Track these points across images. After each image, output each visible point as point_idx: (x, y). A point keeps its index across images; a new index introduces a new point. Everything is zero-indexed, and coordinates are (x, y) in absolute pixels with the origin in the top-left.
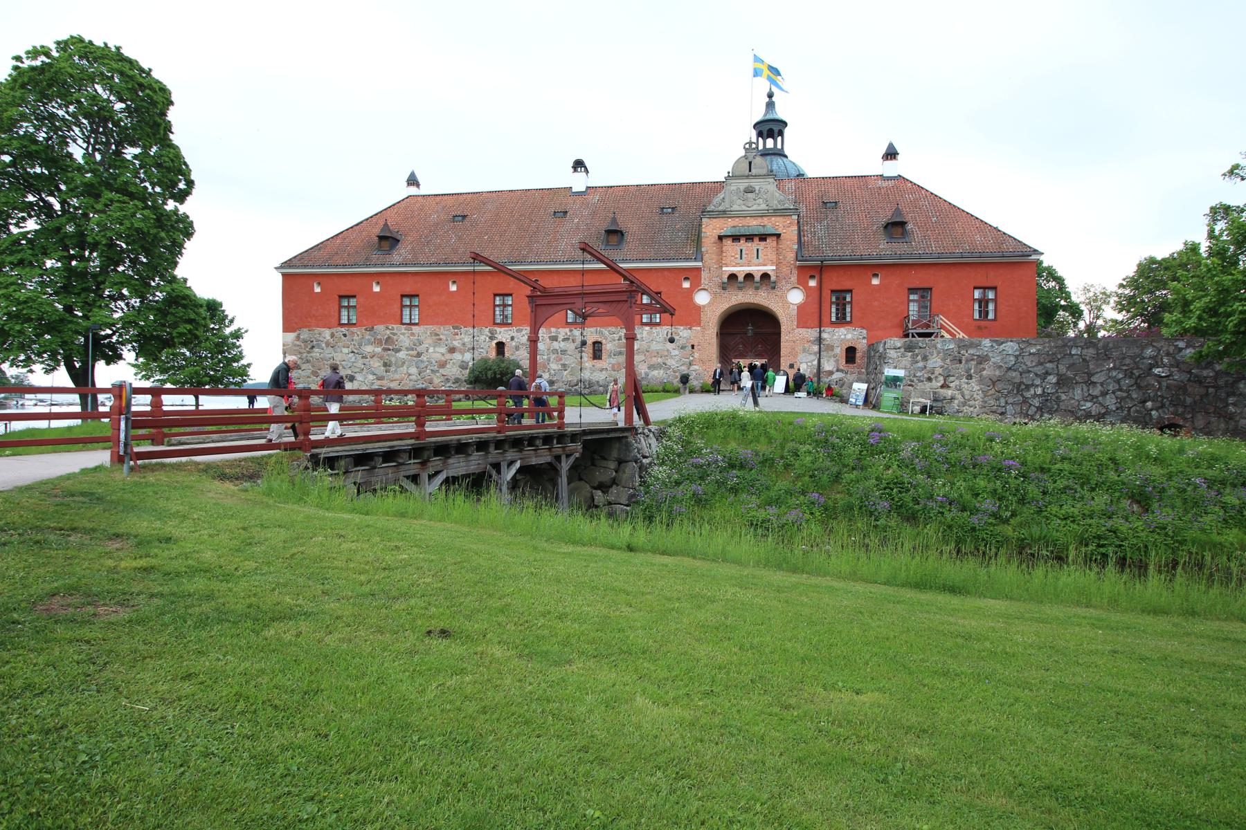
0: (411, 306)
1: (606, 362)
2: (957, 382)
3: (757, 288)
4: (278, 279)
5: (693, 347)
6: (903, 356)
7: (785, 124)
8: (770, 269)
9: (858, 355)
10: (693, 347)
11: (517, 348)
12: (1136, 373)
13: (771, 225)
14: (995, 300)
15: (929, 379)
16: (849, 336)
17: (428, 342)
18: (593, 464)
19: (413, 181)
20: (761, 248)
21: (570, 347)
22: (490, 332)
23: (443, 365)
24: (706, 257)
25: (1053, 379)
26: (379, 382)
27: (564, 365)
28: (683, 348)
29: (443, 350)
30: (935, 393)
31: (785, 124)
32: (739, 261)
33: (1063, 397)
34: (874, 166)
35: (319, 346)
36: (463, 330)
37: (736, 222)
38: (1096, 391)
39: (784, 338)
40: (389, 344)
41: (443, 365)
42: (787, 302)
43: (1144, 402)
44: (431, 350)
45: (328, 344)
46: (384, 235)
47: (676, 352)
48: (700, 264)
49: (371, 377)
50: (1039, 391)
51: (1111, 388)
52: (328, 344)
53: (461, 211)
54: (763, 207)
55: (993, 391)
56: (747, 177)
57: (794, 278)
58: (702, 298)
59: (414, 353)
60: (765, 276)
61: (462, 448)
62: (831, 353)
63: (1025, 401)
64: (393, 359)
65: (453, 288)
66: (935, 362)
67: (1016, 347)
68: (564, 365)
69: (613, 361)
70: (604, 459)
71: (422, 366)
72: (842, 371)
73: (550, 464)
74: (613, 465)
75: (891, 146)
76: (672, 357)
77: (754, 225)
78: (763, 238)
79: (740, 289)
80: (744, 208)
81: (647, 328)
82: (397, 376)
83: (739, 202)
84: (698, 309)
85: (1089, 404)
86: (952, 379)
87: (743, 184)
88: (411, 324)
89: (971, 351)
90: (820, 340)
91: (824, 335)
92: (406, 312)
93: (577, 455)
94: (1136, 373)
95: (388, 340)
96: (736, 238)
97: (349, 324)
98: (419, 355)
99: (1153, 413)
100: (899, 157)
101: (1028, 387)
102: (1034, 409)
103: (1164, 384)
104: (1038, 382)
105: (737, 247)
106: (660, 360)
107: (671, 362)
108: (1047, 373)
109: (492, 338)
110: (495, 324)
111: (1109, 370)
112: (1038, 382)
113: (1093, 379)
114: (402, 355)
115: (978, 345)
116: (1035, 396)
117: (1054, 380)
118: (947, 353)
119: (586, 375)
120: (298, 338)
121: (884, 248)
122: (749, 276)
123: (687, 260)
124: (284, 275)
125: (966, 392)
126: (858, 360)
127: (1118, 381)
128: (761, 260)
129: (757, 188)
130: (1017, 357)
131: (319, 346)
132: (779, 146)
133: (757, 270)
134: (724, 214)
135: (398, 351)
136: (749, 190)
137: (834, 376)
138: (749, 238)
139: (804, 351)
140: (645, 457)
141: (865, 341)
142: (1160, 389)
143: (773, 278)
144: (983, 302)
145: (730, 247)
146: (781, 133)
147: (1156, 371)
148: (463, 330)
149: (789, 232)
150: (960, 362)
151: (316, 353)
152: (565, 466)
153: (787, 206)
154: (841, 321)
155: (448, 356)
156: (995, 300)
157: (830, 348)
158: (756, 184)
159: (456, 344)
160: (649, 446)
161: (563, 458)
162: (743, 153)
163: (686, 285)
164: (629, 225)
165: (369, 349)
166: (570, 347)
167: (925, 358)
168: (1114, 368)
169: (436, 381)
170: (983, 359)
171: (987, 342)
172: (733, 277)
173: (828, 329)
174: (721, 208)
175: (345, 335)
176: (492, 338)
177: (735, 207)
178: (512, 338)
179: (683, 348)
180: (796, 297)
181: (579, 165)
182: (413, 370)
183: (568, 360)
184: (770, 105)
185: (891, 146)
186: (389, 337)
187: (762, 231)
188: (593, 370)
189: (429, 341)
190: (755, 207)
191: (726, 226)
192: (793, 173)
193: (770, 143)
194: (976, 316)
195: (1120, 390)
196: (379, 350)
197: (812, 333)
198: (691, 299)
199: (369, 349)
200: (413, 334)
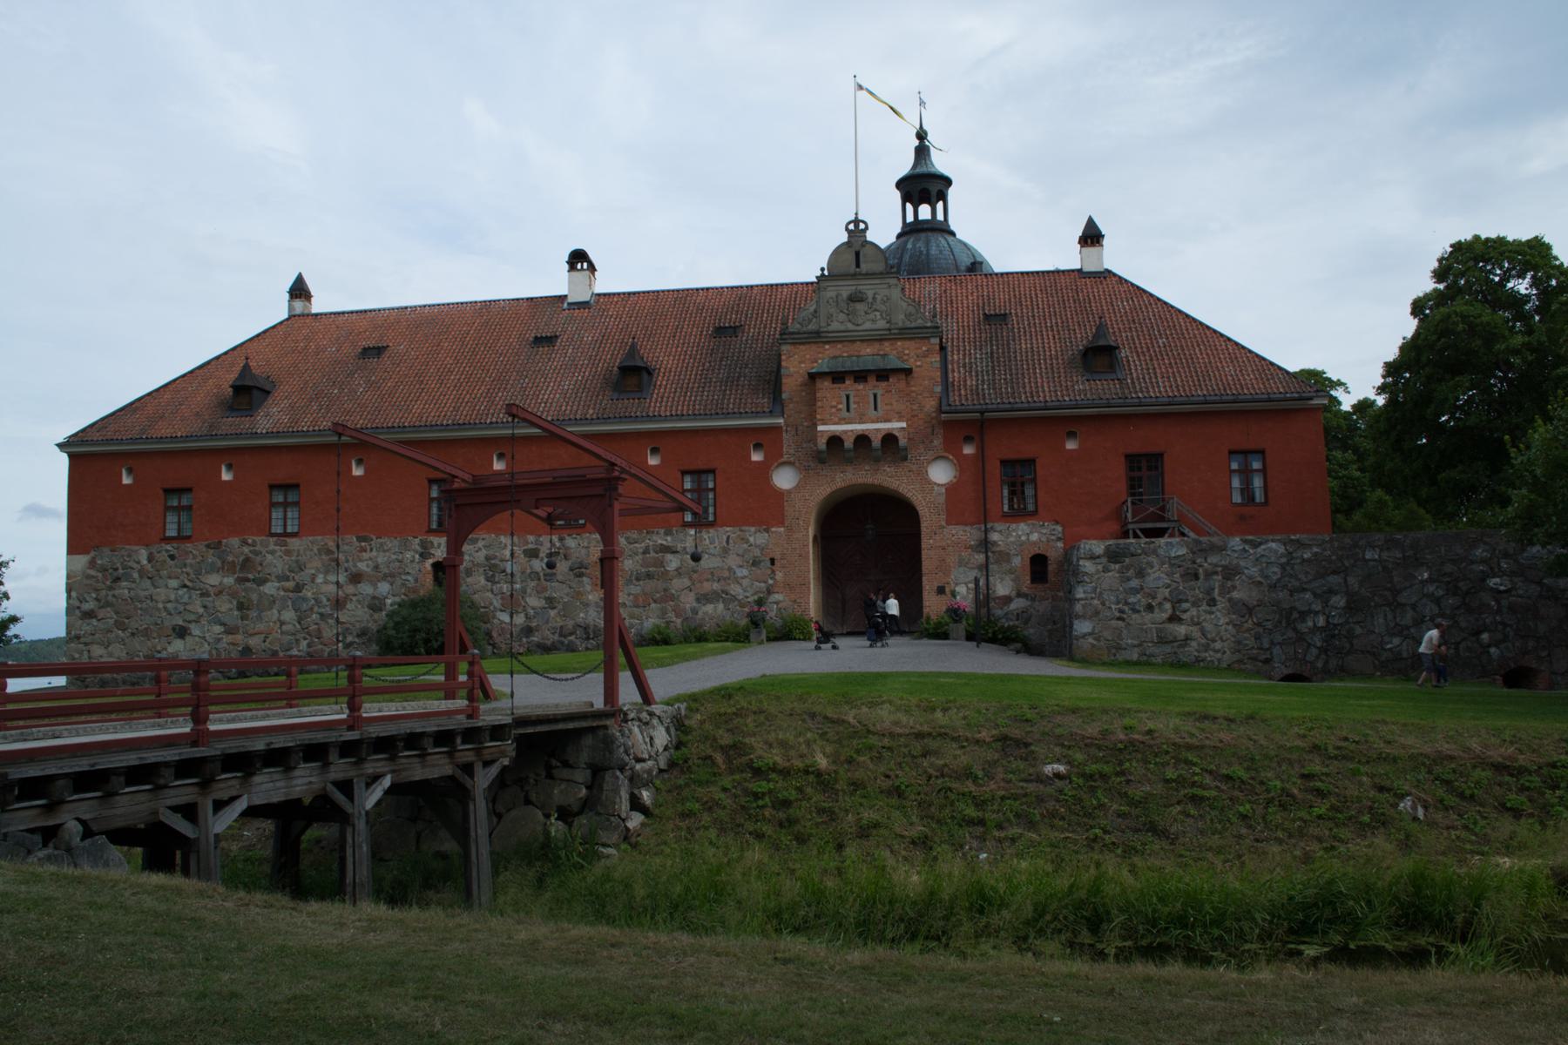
0: (285, 505)
2: (1194, 612)
3: (877, 460)
4: (63, 460)
5: (773, 561)
6: (1106, 570)
7: (948, 182)
8: (896, 425)
9: (1051, 568)
10: (773, 561)
12: (1463, 586)
13: (893, 353)
14: (1264, 471)
15: (1150, 608)
16: (1035, 537)
17: (314, 565)
18: (550, 776)
19: (299, 290)
20: (879, 392)
22: (423, 544)
23: (339, 604)
24: (790, 408)
25: (1339, 601)
26: (227, 639)
27: (551, 602)
28: (755, 563)
30: (1159, 631)
31: (948, 182)
32: (845, 414)
33: (1358, 630)
34: (1069, 257)
35: (128, 577)
36: (375, 542)
37: (838, 350)
38: (1408, 617)
39: (926, 542)
40: (247, 570)
42: (929, 482)
43: (1479, 633)
44: (320, 579)
45: (142, 573)
46: (241, 381)
47: (745, 572)
48: (781, 421)
49: (218, 629)
50: (1321, 621)
51: (1427, 612)
52: (142, 573)
53: (376, 340)
54: (882, 324)
55: (1249, 624)
56: (854, 276)
57: (938, 442)
58: (784, 479)
59: (291, 584)
60: (889, 439)
61: (278, 758)
62: (1005, 566)
63: (1300, 638)
64: (254, 597)
65: (357, 471)
66: (1158, 577)
67: (1282, 550)
68: (551, 602)
69: (635, 590)
70: (566, 764)
71: (305, 607)
72: (1025, 596)
73: (452, 778)
74: (581, 775)
75: (1091, 224)
76: (737, 581)
77: (868, 355)
78: (883, 375)
79: (849, 461)
80: (850, 326)
81: (692, 532)
82: (261, 627)
83: (842, 317)
84: (780, 495)
85: (1396, 641)
86: (1185, 605)
87: (846, 289)
88: (285, 534)
89: (1213, 559)
90: (985, 545)
91: (995, 537)
92: (277, 514)
93: (506, 762)
94: (1463, 586)
95: (247, 563)
96: (838, 377)
97: (181, 538)
98: (298, 588)
99: (1493, 650)
100: (1105, 242)
101: (1303, 615)
102: (1314, 651)
103: (1504, 603)
104: (1317, 607)
106: (716, 586)
107: (735, 589)
108: (1331, 592)
109: (424, 556)
110: (430, 531)
111: (1423, 582)
112: (1317, 607)
113: (1402, 599)
114: (270, 588)
115: (1222, 549)
116: (1316, 628)
117: (1342, 603)
118: (1174, 563)
120: (92, 564)
121: (1084, 390)
122: (862, 440)
123: (757, 414)
124: (72, 457)
125: (1208, 626)
126: (1051, 577)
127: (1438, 601)
128: (881, 412)
129: (870, 294)
130: (1283, 566)
131: (128, 577)
132: (940, 217)
133: (875, 427)
134: (816, 337)
135: (262, 582)
136: (855, 298)
137: (1013, 606)
138: (861, 376)
139: (962, 563)
140: (639, 760)
141: (1060, 544)
142: (1499, 611)
143: (903, 442)
144: (1246, 473)
146: (942, 196)
147: (1493, 582)
148: (375, 542)
149: (926, 364)
150: (1196, 577)
151: (123, 590)
152: (483, 779)
153: (920, 322)
154: (1018, 513)
155: (350, 589)
156: (1264, 471)
157: (1004, 557)
158: (869, 288)
159: (362, 566)
160: (649, 742)
161: (478, 768)
162: (844, 237)
163: (757, 457)
164: (663, 357)
167: (1141, 574)
168: (1431, 580)
169: (329, 632)
170: (1230, 572)
171: (1235, 542)
172: (835, 441)
173: (999, 526)
174: (812, 327)
175: (172, 557)
177: (835, 326)
179: (755, 563)
180: (941, 474)
181: (578, 258)
182: (289, 615)
183: (559, 591)
184: (922, 152)
185: (1091, 224)
186: (247, 560)
187: (881, 364)
189: (317, 563)
190: (868, 325)
191: (823, 358)
192: (966, 261)
193: (925, 212)
194: (1237, 498)
195: (1443, 615)
196: (229, 581)
197: (968, 534)
198: (767, 479)
199: (213, 579)
200: (288, 553)
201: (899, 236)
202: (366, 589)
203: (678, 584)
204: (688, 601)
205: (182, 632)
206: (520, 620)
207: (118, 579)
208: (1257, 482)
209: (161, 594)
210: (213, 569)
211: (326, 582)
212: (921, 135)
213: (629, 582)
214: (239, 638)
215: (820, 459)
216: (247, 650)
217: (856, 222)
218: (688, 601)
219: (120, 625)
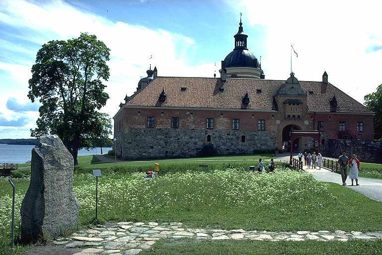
1: (246, 143)
11: (215, 137)
21: (234, 137)
23: (187, 143)
27: (232, 144)
29: (188, 138)
41: (187, 143)
44: (183, 138)
59: (177, 138)
64: (169, 141)
68: (232, 144)
87: (291, 86)
105: (290, 106)
114: (172, 139)
119: (240, 147)
143: (301, 117)
145: (288, 107)
158: (294, 86)
162: (290, 76)
165: (159, 137)
166: (234, 137)
169: (185, 149)
176: (206, 134)
177: (288, 93)
178: (213, 134)
179: (272, 138)
183: (234, 142)
184: (241, 29)
188: (242, 145)
196: (163, 137)
199: (159, 137)
201: (234, 50)
202: (193, 140)
203: (257, 142)
204: (259, 145)
205: (152, 148)
206: (226, 147)
207: (137, 136)
208: (361, 128)
209: (147, 139)
210: (159, 134)
211: (185, 138)
212: (241, 24)
213: (248, 141)
214: (165, 149)
215: (285, 118)
216: (167, 152)
217: (292, 73)
218: (259, 145)
219: (137, 145)
